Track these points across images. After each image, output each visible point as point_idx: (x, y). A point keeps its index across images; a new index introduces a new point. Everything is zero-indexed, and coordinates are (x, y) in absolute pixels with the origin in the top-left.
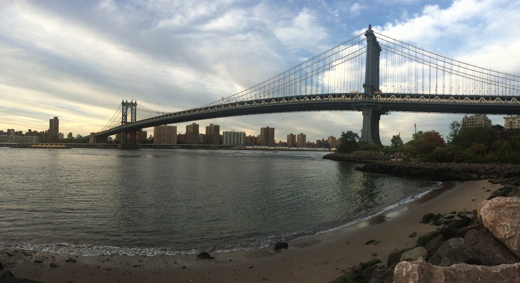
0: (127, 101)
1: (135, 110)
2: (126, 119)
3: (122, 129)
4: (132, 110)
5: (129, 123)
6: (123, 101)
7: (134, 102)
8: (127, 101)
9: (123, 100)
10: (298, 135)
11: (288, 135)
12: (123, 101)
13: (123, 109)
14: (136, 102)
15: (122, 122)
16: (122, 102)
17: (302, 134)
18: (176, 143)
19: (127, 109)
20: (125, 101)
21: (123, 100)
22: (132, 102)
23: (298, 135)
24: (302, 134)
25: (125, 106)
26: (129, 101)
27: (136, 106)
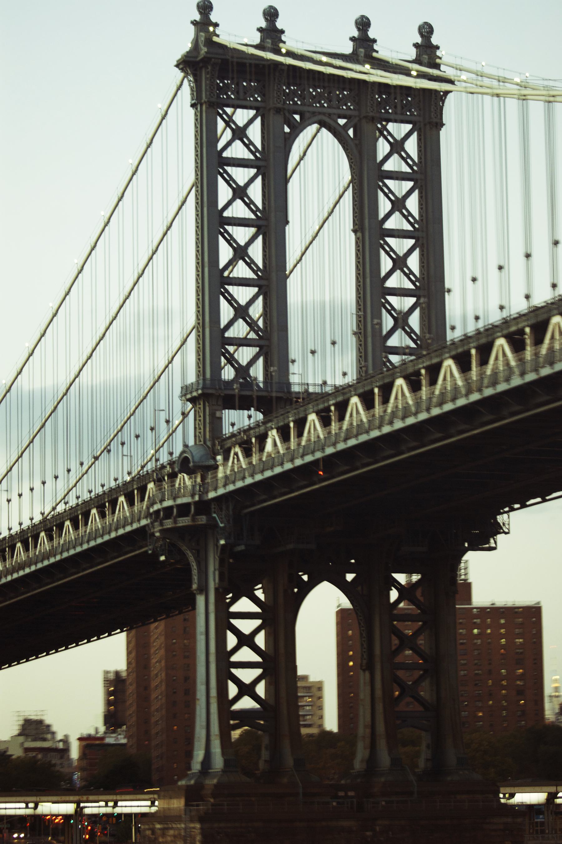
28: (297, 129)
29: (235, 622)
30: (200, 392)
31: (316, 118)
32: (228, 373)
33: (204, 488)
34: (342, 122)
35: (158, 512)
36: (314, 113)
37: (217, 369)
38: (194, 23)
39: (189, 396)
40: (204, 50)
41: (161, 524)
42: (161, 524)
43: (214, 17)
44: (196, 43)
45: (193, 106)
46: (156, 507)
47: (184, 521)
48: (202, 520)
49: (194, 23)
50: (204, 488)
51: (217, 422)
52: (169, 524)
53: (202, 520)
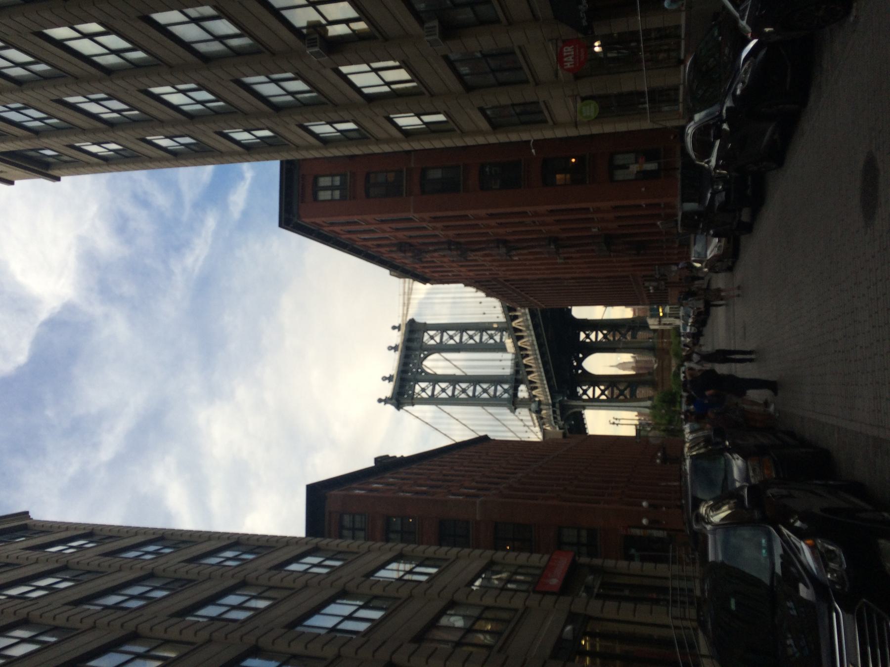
0: (390, 379)
1: (442, 328)
2: (495, 380)
3: (553, 405)
4: (441, 348)
6: (386, 401)
7: (397, 338)
9: (380, 401)
12: (386, 401)
13: (433, 400)
15: (514, 403)
16: (390, 408)
19: (435, 379)
20: (387, 389)
21: (380, 401)
22: (395, 348)
26: (391, 363)
27: (426, 327)
28: (423, 371)
29: (596, 396)
30: (512, 405)
31: (420, 364)
32: (506, 396)
33: (548, 404)
34: (422, 356)
35: (555, 422)
36: (418, 365)
37: (505, 399)
38: (385, 404)
39: (514, 410)
40: (394, 401)
41: (559, 421)
42: (559, 421)
43: (383, 398)
44: (392, 404)
45: (413, 405)
46: (553, 422)
47: (558, 412)
48: (557, 405)
49: (385, 404)
50: (548, 404)
51: (523, 399)
52: (559, 418)
53: (557, 405)
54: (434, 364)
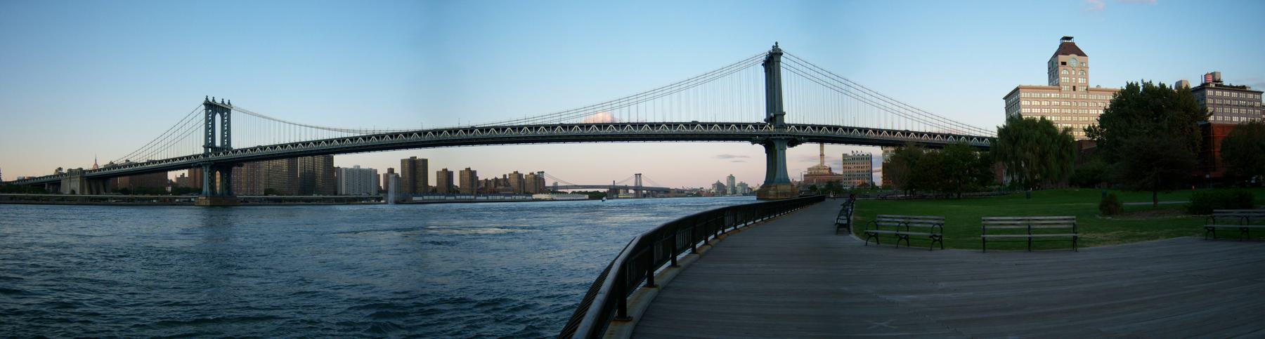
0: (214, 100)
2: (214, 140)
5: (218, 148)
6: (207, 99)
8: (214, 100)
9: (207, 97)
10: (461, 172)
11: (438, 172)
12: (207, 99)
14: (229, 103)
15: (206, 147)
17: (446, 169)
18: (263, 193)
20: (211, 100)
22: (223, 102)
23: (461, 172)
24: (446, 169)
25: (210, 111)
54: (218, 117)
